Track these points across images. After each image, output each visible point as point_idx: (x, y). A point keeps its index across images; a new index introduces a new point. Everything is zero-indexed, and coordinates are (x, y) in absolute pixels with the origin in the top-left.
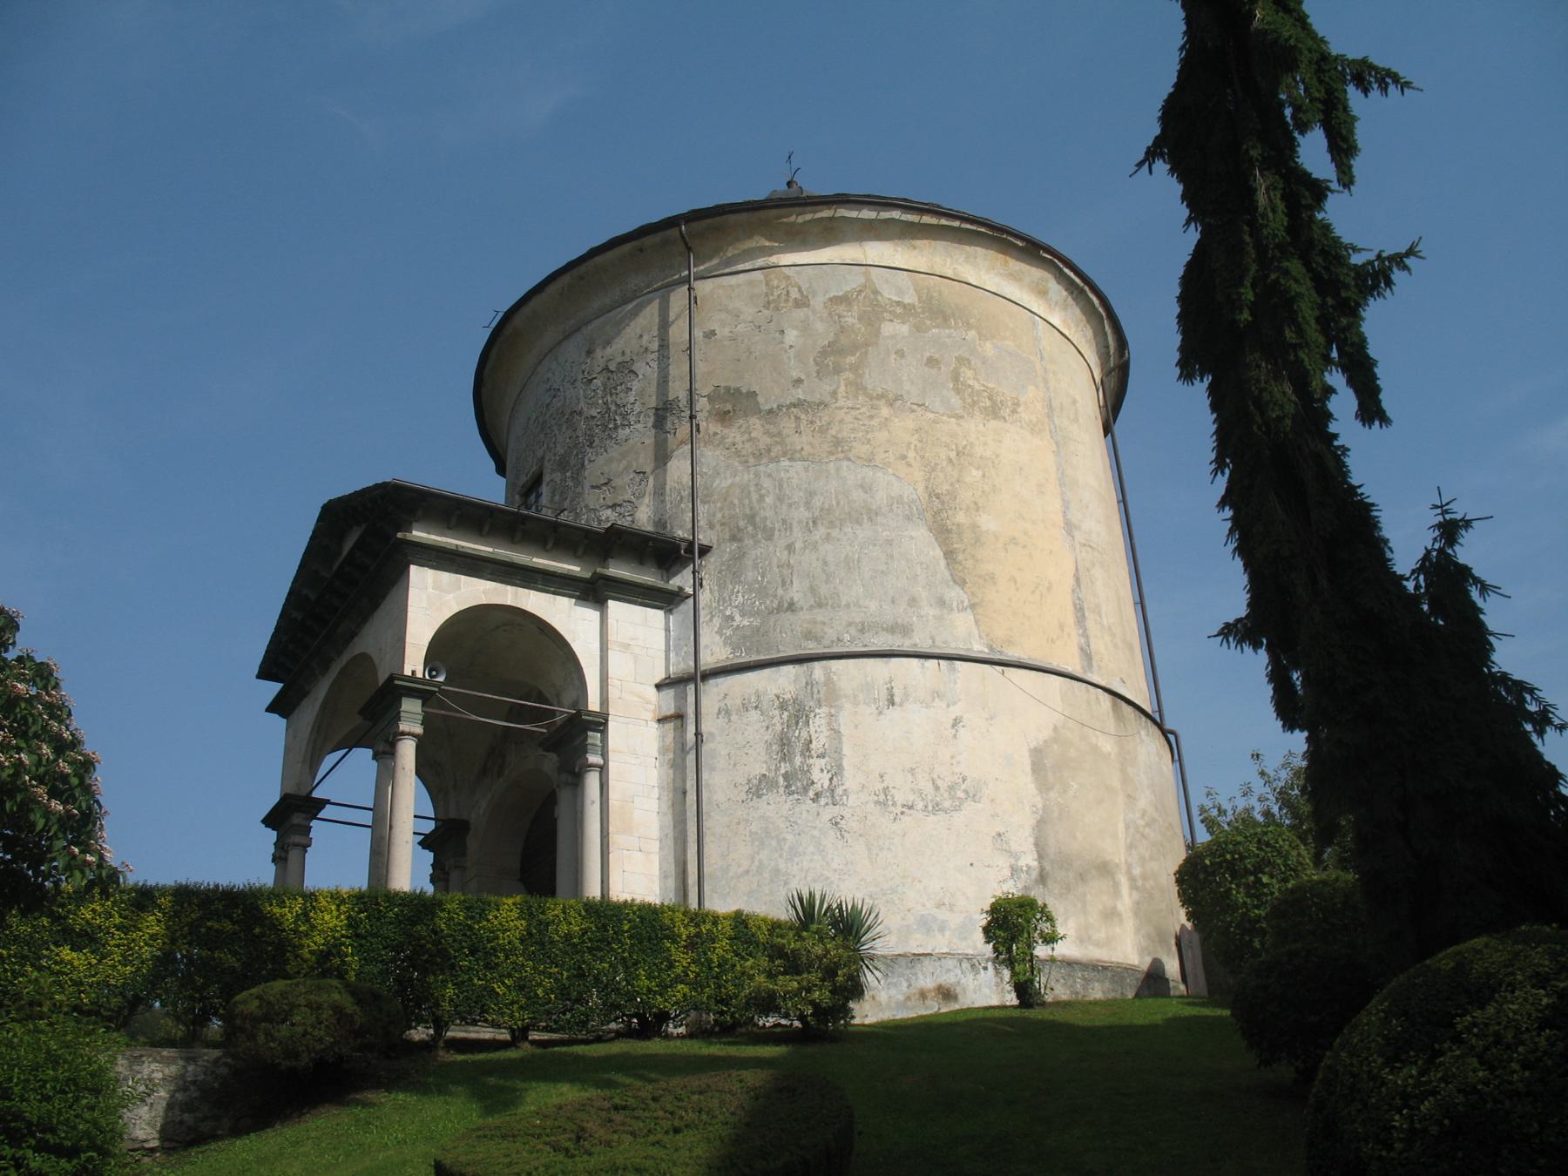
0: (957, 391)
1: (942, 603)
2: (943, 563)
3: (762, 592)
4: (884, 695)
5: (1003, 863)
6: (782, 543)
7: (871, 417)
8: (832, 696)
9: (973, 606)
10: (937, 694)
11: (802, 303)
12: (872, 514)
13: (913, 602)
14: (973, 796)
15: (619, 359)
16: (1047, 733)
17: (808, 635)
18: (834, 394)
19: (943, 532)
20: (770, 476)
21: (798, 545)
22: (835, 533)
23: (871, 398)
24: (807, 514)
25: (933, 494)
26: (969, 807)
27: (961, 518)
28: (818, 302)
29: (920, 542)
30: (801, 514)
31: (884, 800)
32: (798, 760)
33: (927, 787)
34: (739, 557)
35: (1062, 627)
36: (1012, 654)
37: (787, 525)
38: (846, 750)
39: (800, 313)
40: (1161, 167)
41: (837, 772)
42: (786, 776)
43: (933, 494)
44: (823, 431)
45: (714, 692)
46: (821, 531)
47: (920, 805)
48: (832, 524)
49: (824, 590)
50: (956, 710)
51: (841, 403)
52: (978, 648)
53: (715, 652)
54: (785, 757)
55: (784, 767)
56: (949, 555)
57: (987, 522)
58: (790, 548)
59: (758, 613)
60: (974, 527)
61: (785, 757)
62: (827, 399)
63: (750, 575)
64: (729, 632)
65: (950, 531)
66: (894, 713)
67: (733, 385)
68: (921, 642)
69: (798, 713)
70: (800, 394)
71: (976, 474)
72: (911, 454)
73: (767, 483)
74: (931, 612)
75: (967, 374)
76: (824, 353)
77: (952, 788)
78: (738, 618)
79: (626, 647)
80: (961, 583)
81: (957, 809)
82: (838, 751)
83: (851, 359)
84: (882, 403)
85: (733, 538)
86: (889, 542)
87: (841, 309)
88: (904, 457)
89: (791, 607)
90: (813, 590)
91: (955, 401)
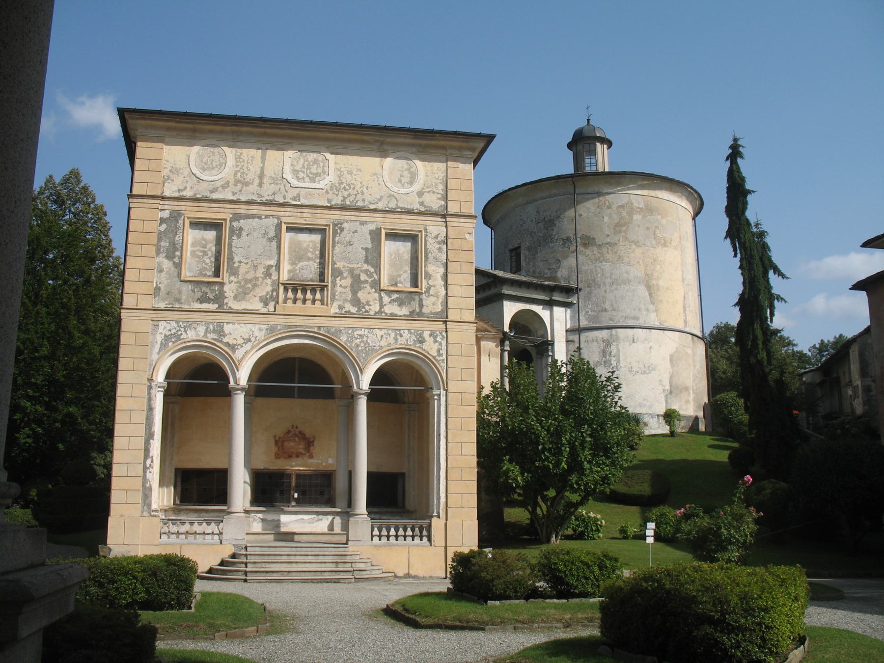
0: (655, 238)
1: (648, 310)
2: (648, 297)
3: (597, 305)
4: (632, 339)
5: (661, 388)
6: (603, 290)
7: (630, 249)
8: (617, 339)
9: (656, 311)
10: (646, 339)
11: (609, 207)
12: (629, 281)
13: (640, 310)
14: (654, 369)
15: (549, 218)
16: (674, 350)
17: (611, 319)
18: (619, 240)
19: (649, 287)
20: (599, 267)
21: (608, 291)
22: (619, 287)
23: (630, 242)
24: (611, 281)
25: (647, 275)
26: (653, 372)
27: (654, 282)
28: (614, 207)
29: (642, 291)
30: (608, 280)
31: (631, 370)
32: (608, 357)
33: (642, 367)
34: (590, 293)
35: (679, 314)
36: (666, 325)
37: (605, 284)
38: (621, 355)
39: (609, 211)
40: (738, 308)
41: (618, 361)
42: (604, 362)
43: (647, 275)
44: (616, 253)
45: (584, 336)
46: (614, 287)
47: (640, 372)
48: (618, 284)
49: (615, 305)
50: (651, 344)
51: (621, 243)
52: (657, 324)
53: (584, 323)
54: (604, 356)
55: (604, 359)
56: (650, 294)
57: (661, 283)
58: (605, 291)
59: (596, 311)
60: (658, 285)
61: (604, 356)
62: (617, 242)
63: (594, 299)
64: (587, 316)
65: (651, 287)
66: (633, 344)
67: (589, 234)
68: (641, 322)
69: (608, 343)
70: (608, 240)
71: (659, 267)
72: (641, 261)
73: (598, 269)
74: (645, 313)
75: (658, 231)
76: (616, 226)
77: (649, 367)
78: (590, 312)
79: (558, 319)
80: (653, 303)
81: (650, 373)
82: (619, 355)
83: (624, 228)
84: (633, 244)
85: (588, 286)
86: (634, 291)
87: (621, 210)
88: (639, 262)
89: (606, 310)
90: (612, 305)
91: (654, 242)
